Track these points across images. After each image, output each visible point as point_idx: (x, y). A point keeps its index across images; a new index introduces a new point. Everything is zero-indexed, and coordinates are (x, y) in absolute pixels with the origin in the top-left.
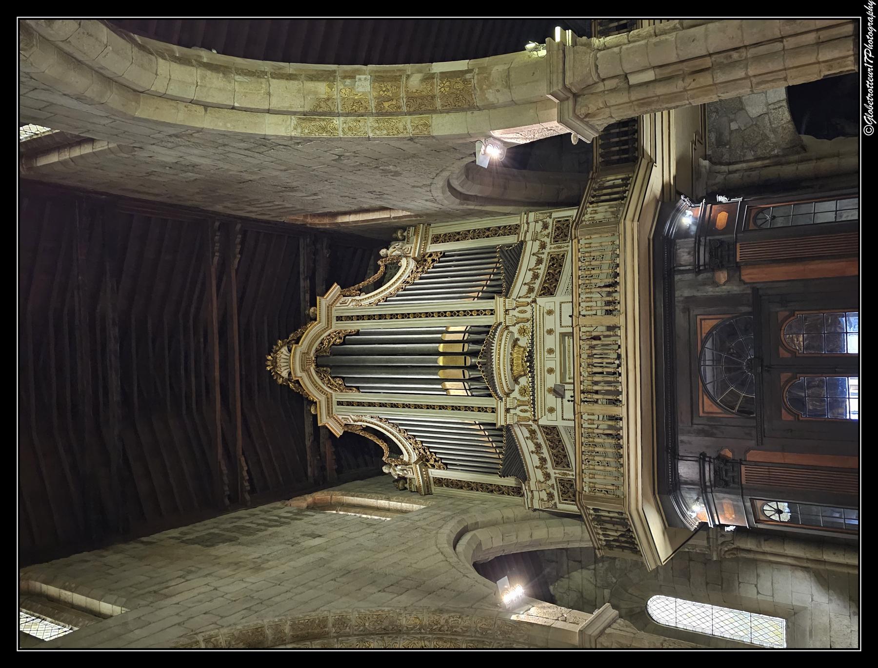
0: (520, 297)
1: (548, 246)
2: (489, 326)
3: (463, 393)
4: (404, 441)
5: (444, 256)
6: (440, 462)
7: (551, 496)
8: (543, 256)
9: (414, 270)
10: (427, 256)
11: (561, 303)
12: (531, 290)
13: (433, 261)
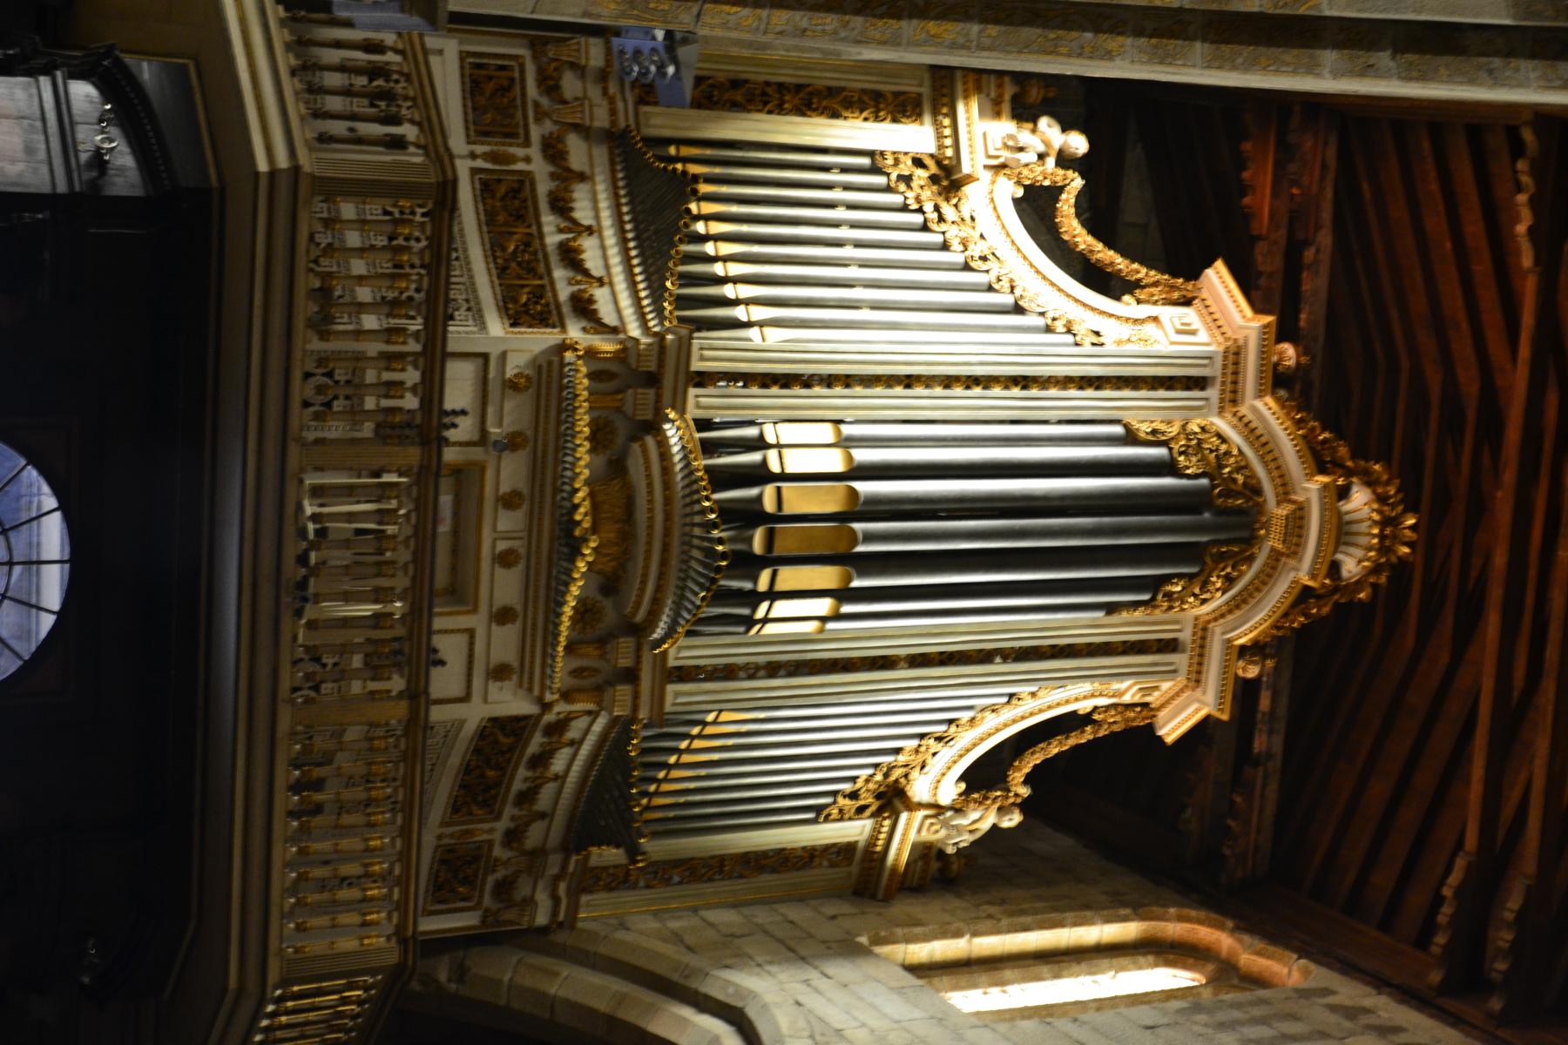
0: (589, 713)
1: (497, 837)
2: (689, 633)
3: (788, 433)
4: (1004, 250)
5: (818, 809)
6: (894, 177)
7: (549, 85)
8: (516, 812)
9: (915, 774)
10: (873, 808)
11: (466, 698)
13: (854, 795)
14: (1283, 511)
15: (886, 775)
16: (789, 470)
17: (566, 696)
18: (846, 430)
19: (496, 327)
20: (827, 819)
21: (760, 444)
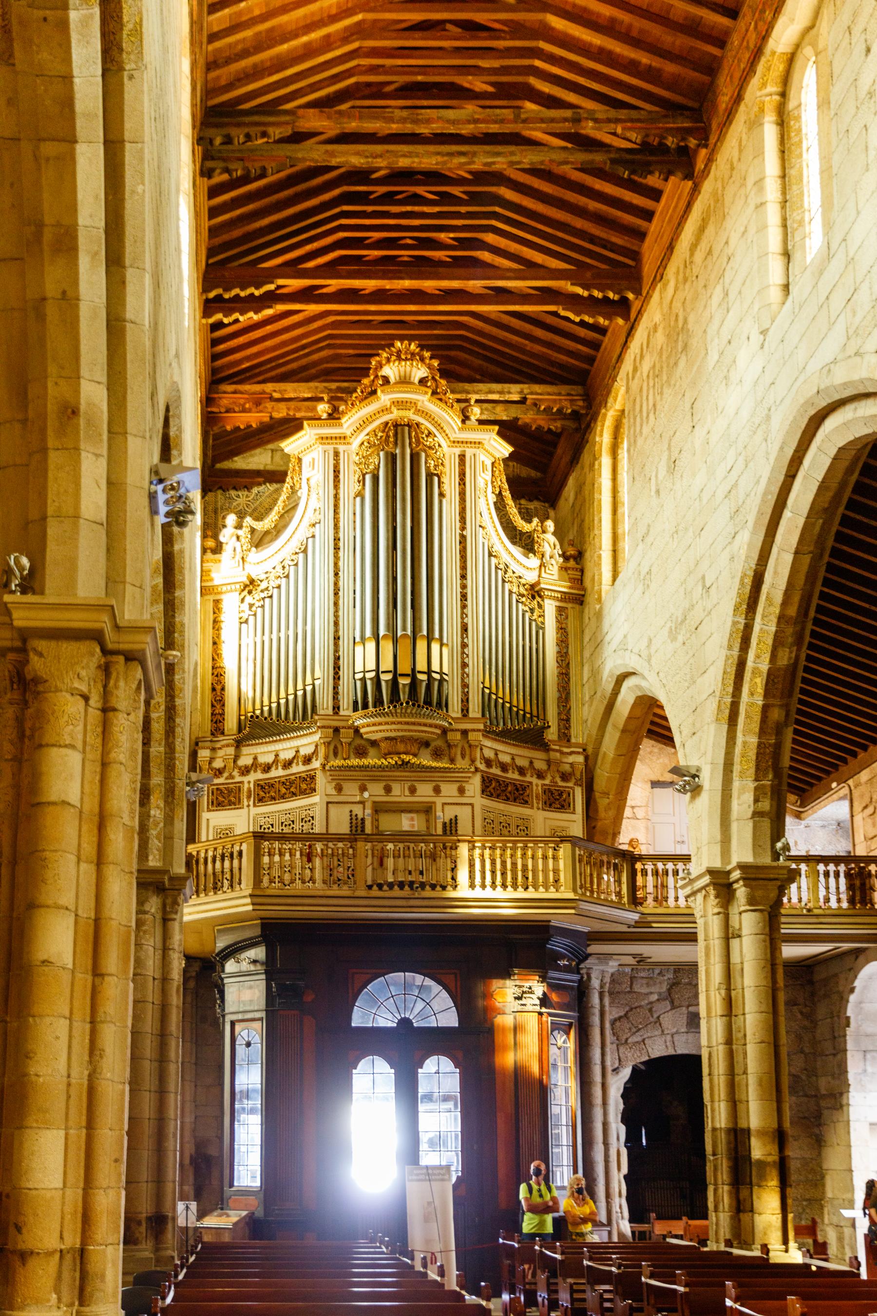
3: (359, 667)
5: (538, 628)
8: (528, 775)
9: (523, 581)
10: (539, 600)
11: (472, 805)
12: (488, 763)
13: (532, 611)
14: (394, 409)
15: (523, 596)
16: (374, 668)
17: (473, 761)
18: (358, 639)
19: (315, 799)
20: (543, 623)
21: (363, 680)
